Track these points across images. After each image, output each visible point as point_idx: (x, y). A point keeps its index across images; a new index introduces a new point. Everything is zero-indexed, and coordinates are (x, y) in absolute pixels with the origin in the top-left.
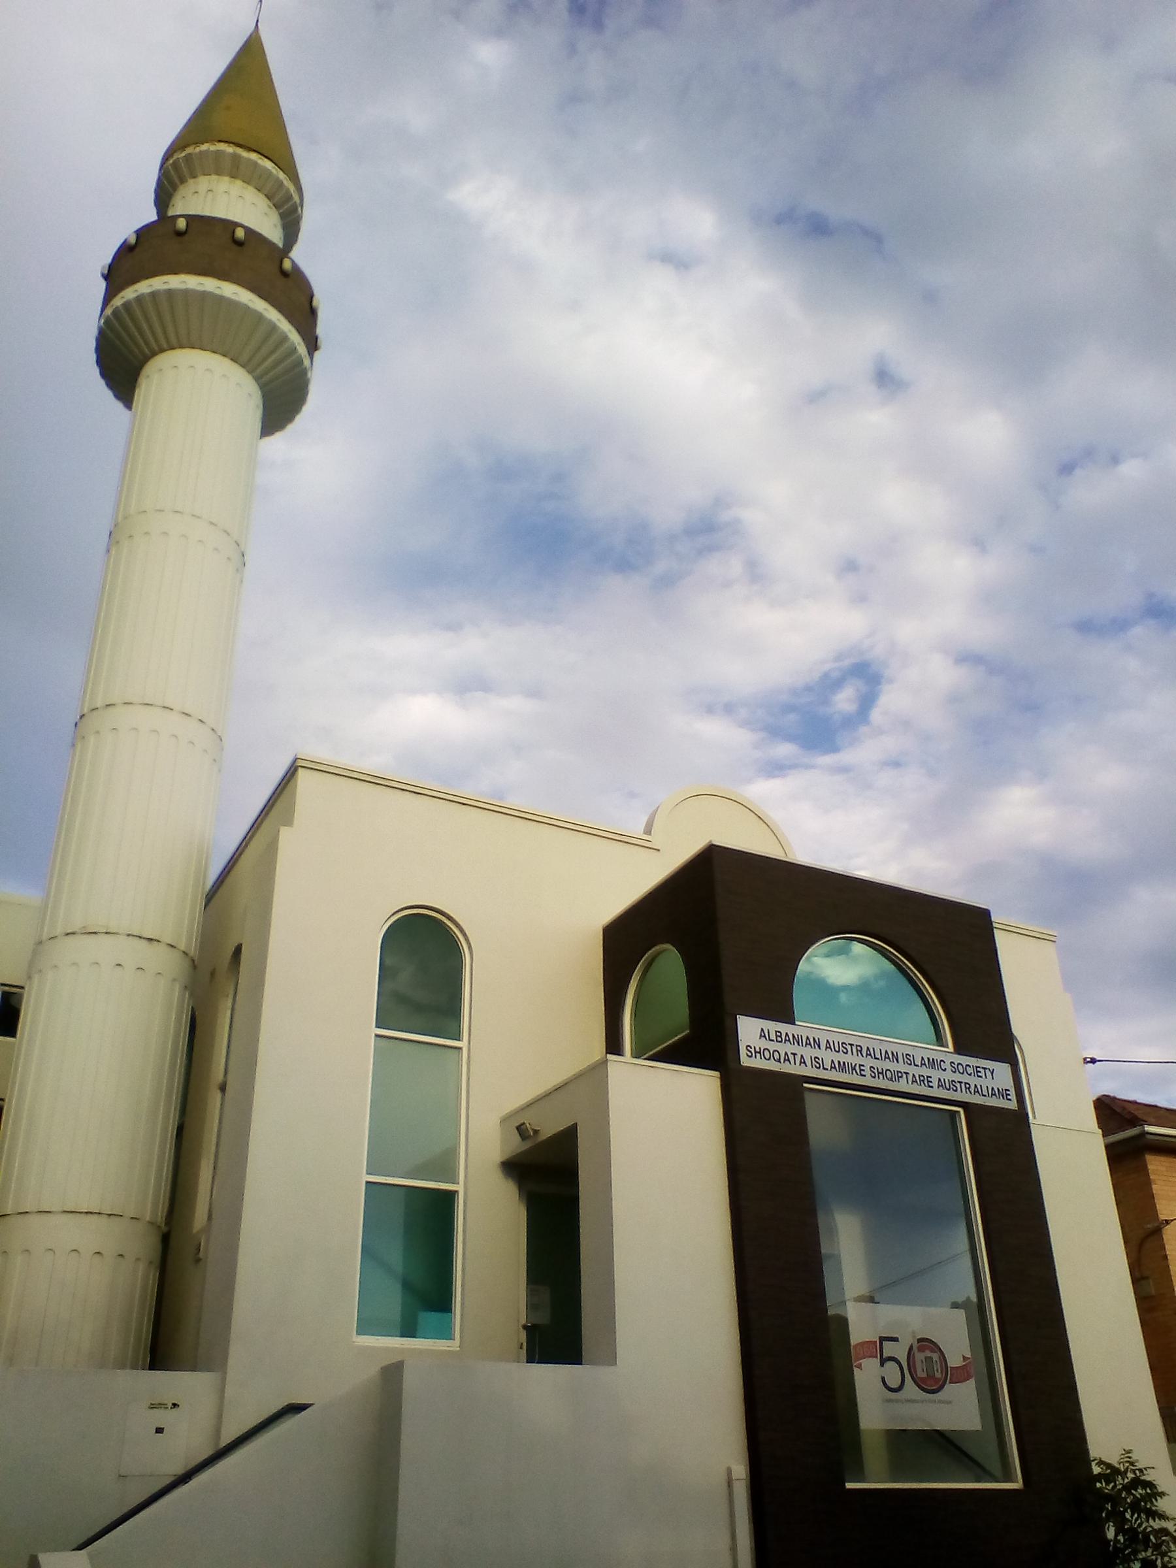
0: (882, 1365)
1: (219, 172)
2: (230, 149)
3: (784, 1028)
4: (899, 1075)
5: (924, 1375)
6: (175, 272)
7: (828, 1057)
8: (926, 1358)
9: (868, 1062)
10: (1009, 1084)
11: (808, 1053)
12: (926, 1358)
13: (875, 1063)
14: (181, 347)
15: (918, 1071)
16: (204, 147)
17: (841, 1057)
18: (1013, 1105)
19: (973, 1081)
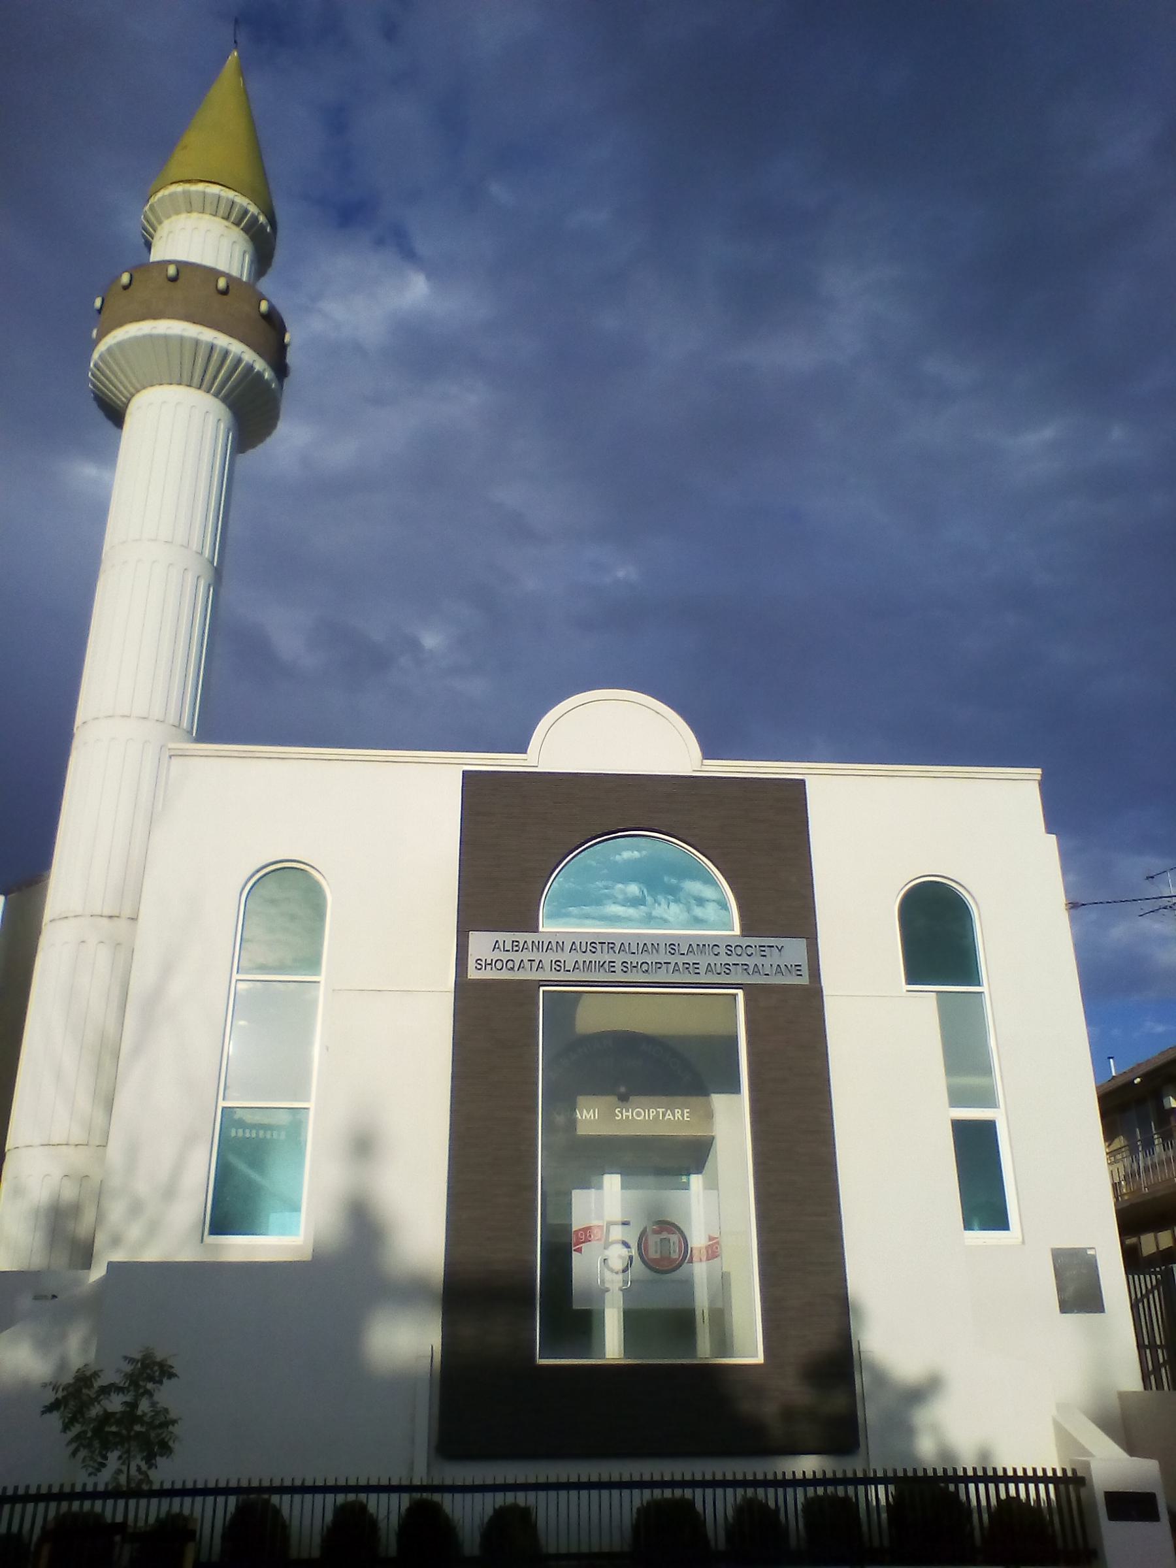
1: (178, 212)
2: (179, 188)
3: (521, 937)
5: (658, 1256)
6: (120, 324)
7: (569, 959)
8: (661, 1240)
9: (619, 959)
10: (802, 959)
11: (548, 958)
12: (661, 1240)
13: (629, 958)
14: (144, 388)
16: (160, 195)
17: (588, 957)
18: (805, 980)
19: (757, 960)
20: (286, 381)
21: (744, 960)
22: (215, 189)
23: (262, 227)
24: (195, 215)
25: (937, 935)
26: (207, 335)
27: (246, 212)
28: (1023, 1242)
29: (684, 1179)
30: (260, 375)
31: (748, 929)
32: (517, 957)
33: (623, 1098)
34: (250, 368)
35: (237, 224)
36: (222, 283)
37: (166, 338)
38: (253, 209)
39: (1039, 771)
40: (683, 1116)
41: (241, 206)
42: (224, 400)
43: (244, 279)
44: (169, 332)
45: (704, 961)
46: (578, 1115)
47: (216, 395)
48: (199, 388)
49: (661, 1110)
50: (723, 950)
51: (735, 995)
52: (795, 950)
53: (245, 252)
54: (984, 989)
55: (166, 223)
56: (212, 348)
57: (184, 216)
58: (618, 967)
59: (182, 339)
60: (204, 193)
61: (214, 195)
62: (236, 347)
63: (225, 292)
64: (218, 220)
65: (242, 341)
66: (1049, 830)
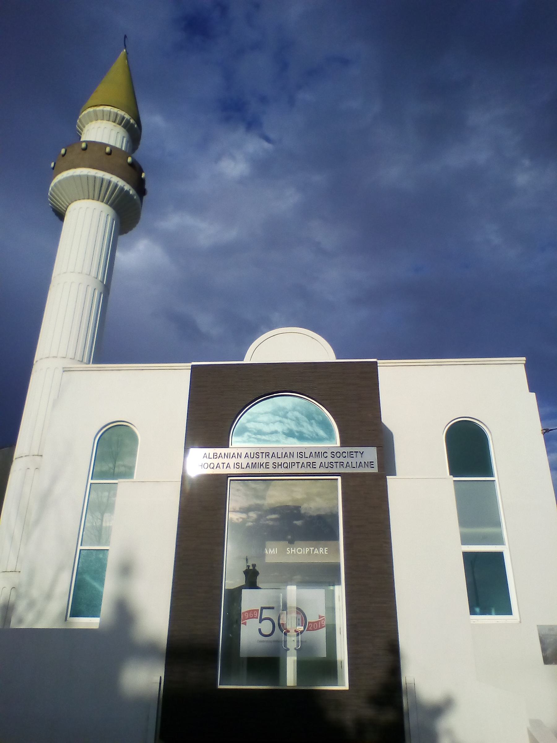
0: (260, 622)
1: (91, 121)
4: (293, 464)
6: (60, 172)
9: (271, 461)
15: (305, 461)
17: (255, 460)
19: (350, 460)
20: (145, 198)
21: (341, 459)
22: (108, 108)
23: (132, 125)
24: (99, 121)
25: (468, 449)
26: (100, 174)
27: (123, 118)
28: (520, 622)
29: (331, 588)
30: (127, 192)
31: (344, 443)
32: (216, 461)
33: (291, 542)
34: (122, 189)
35: (120, 124)
36: (108, 149)
37: (80, 177)
38: (127, 116)
39: (524, 358)
40: (324, 551)
41: (121, 115)
42: (111, 205)
43: (123, 149)
44: (82, 174)
45: (318, 461)
46: (266, 552)
47: (107, 203)
48: (98, 200)
49: (312, 549)
50: (329, 455)
51: (337, 479)
52: (370, 454)
53: (124, 137)
54: (495, 478)
55: (87, 126)
56: (103, 180)
57: (94, 122)
58: (271, 465)
59: (88, 177)
60: (103, 111)
61: (108, 111)
62: (115, 179)
63: (110, 154)
64: (110, 123)
65: (118, 176)
66: (531, 390)
